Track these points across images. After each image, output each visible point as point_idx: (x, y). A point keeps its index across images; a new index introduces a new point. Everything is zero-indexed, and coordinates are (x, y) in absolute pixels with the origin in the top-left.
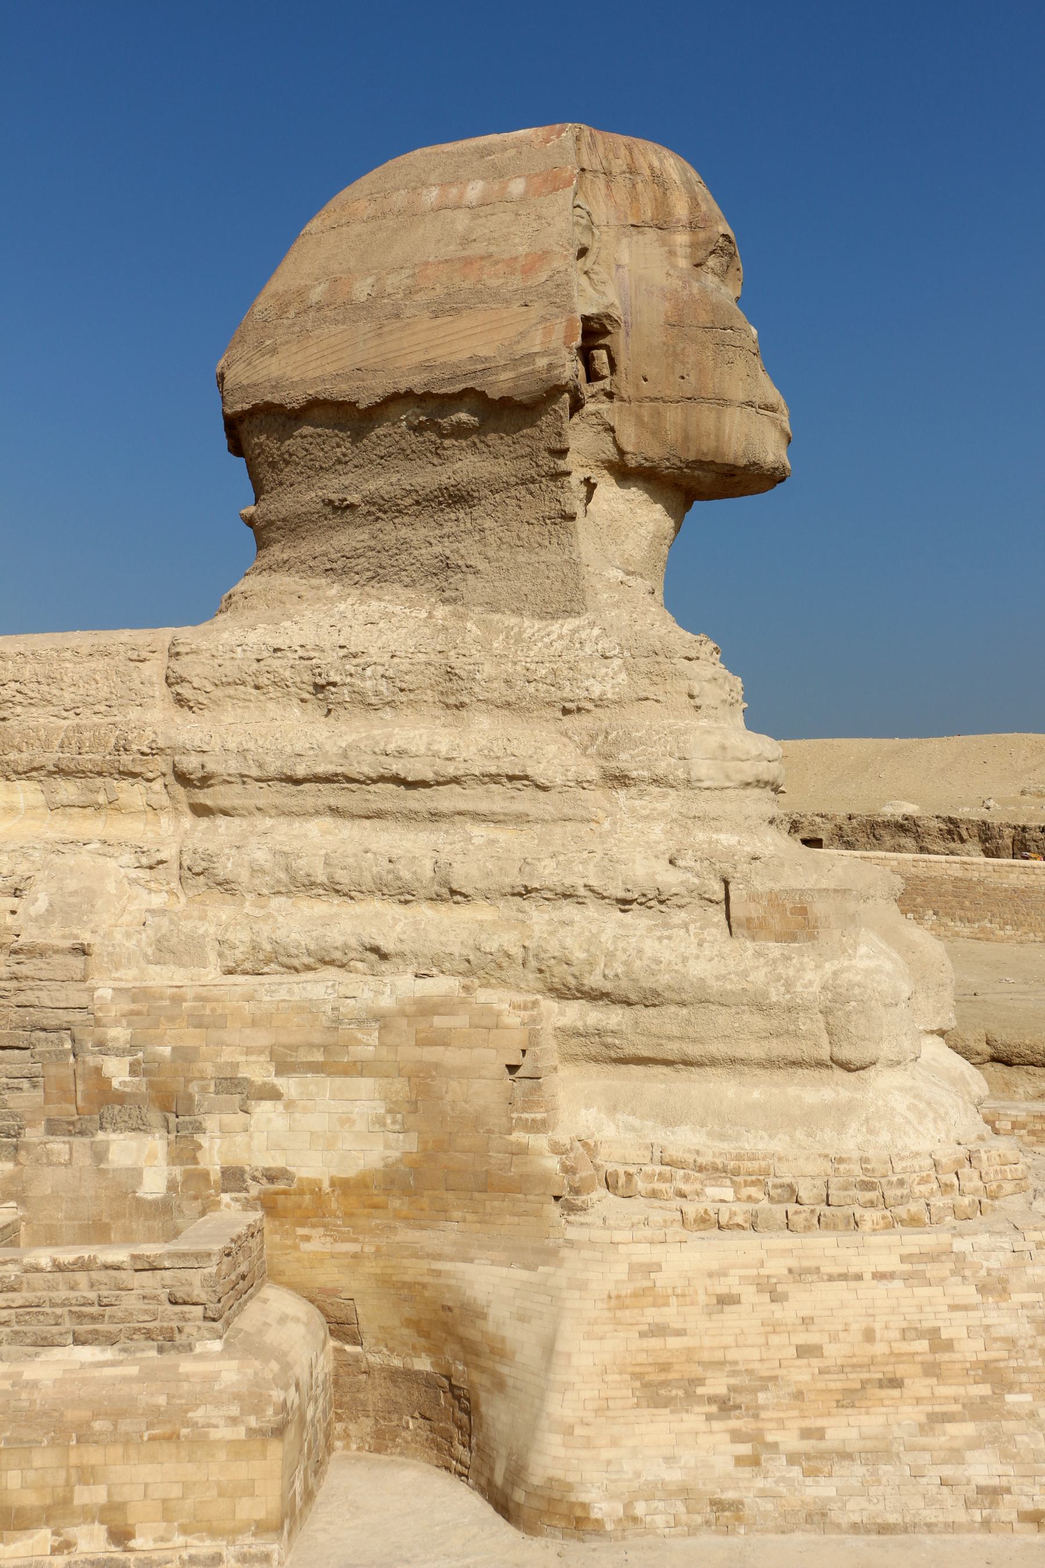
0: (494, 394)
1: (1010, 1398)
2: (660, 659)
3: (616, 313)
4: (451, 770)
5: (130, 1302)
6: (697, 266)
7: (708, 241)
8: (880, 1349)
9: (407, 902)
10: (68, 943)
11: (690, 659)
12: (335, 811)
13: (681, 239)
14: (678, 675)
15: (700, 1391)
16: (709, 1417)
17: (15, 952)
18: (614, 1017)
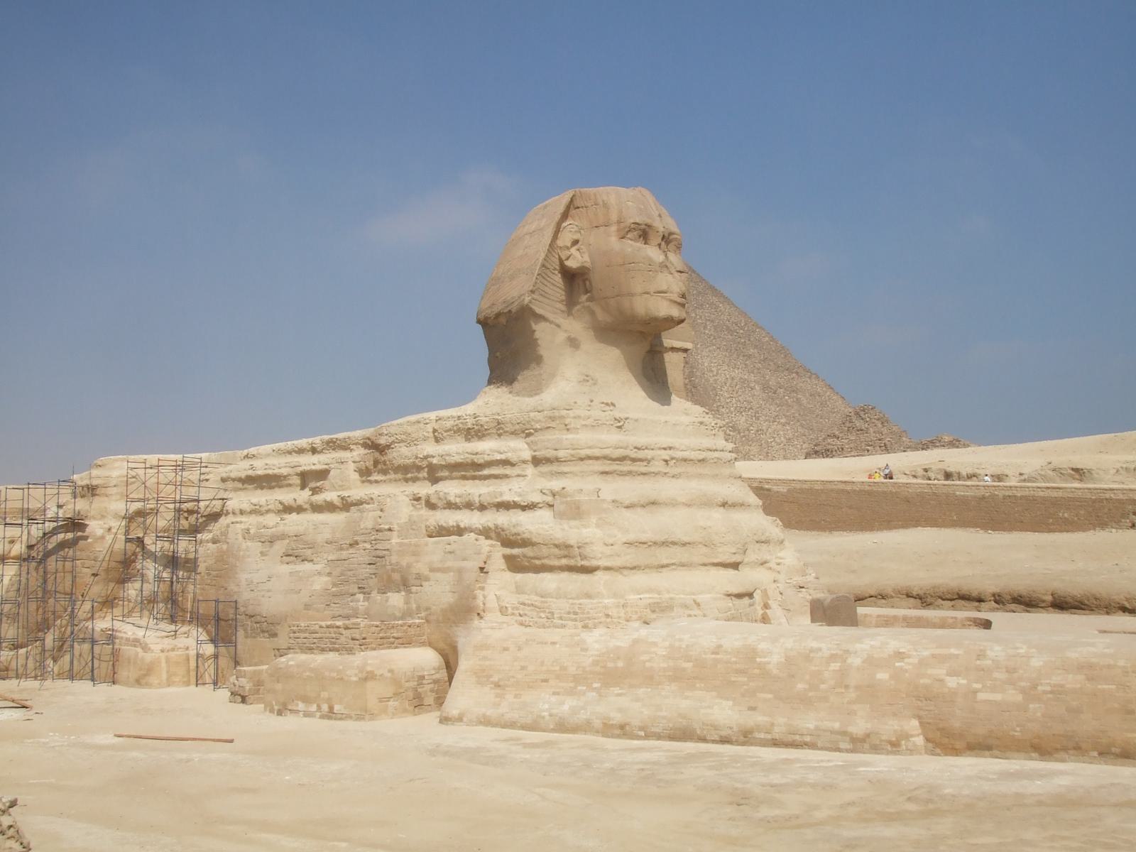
0: (514, 311)
1: (579, 688)
2: (554, 411)
3: (585, 264)
4: (487, 458)
5: (343, 639)
6: (622, 238)
7: (625, 228)
8: (544, 668)
9: (472, 510)
10: (387, 527)
11: (568, 410)
12: (464, 478)
13: (614, 228)
14: (562, 417)
15: (491, 679)
16: (491, 688)
17: (377, 531)
18: (516, 551)
